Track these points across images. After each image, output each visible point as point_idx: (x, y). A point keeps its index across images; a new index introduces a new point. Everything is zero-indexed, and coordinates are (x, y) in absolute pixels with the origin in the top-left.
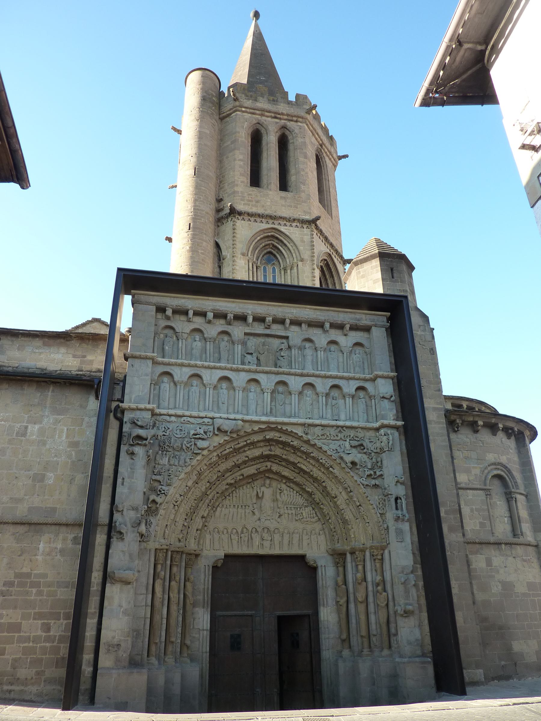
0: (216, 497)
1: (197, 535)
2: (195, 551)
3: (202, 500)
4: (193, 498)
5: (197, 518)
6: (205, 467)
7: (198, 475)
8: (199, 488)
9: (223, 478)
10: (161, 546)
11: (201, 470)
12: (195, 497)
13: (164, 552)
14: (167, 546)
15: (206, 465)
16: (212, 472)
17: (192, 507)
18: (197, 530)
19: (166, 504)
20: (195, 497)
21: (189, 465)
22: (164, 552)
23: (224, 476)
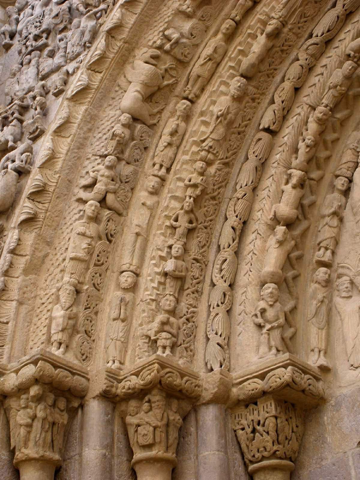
0: (313, 126)
1: (262, 304)
2: (262, 377)
3: (247, 159)
4: (187, 157)
5: (250, 237)
6: (187, 26)
7: (168, 62)
8: (202, 114)
9: (311, 41)
10: (17, 372)
11: (168, 39)
12: (195, 149)
13: (39, 399)
14: (35, 363)
15: (188, 16)
16: (239, 39)
17: (189, 191)
18: (263, 284)
19: (28, 204)
20: (195, 149)
21: (94, 34)
22: (39, 399)
23: (311, 36)
